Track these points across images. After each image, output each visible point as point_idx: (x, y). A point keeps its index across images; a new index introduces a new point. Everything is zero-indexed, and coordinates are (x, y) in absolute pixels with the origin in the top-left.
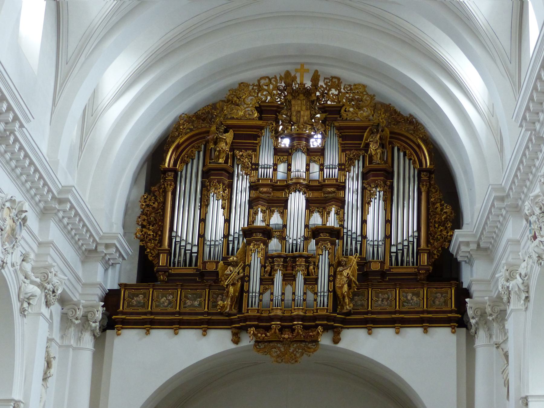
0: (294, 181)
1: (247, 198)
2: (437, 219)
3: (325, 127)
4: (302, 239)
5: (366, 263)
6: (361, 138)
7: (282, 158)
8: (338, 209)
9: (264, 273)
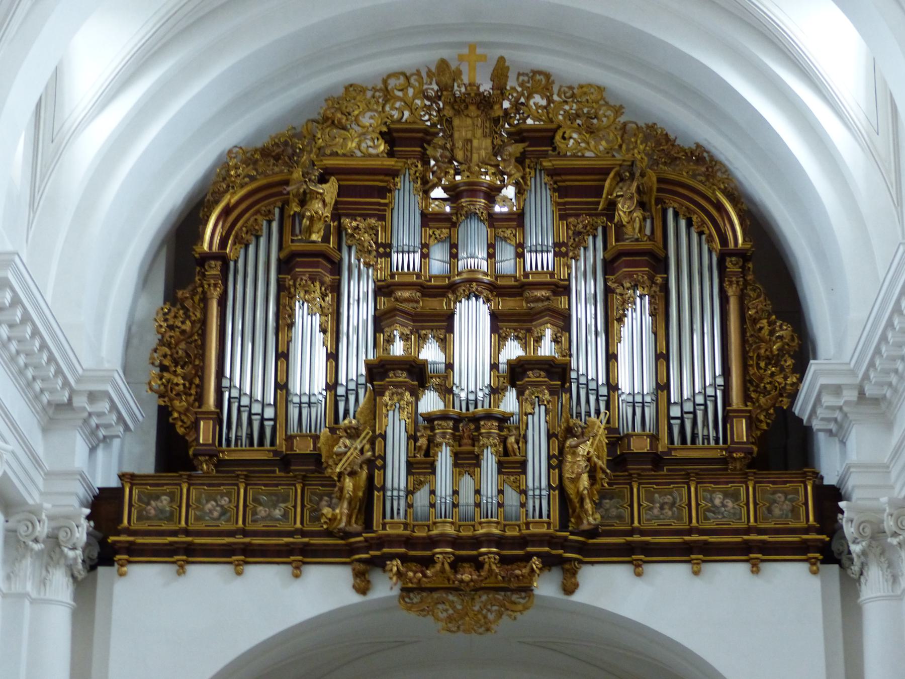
0: (465, 276)
1: (371, 312)
2: (762, 351)
3: (524, 169)
4: (487, 391)
5: (621, 439)
6: (597, 191)
7: (437, 232)
8: (558, 332)
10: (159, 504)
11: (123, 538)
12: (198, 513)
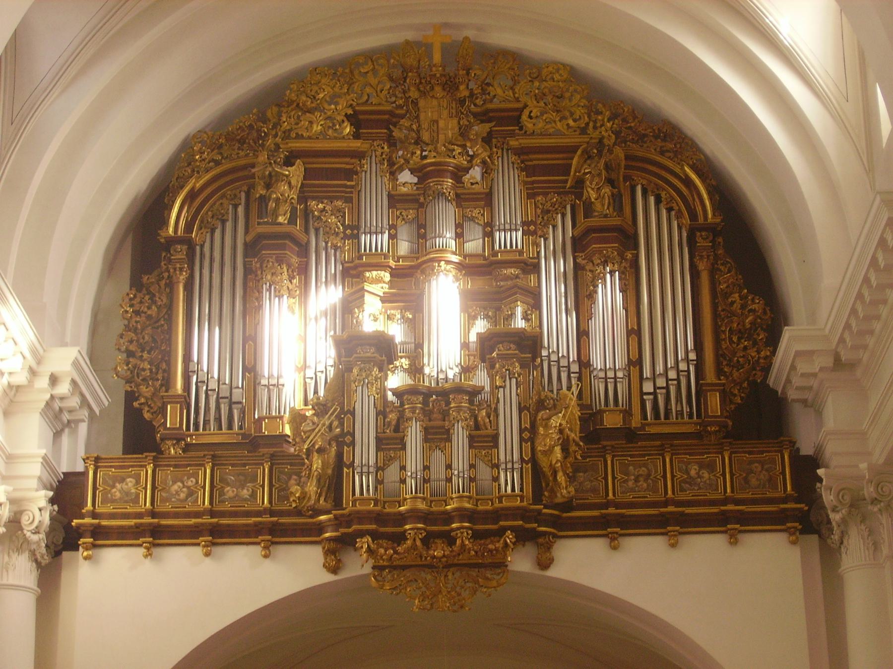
6: (565, 170)
9: (384, 426)
10: (124, 486)
11: (88, 520)
12: (164, 495)
